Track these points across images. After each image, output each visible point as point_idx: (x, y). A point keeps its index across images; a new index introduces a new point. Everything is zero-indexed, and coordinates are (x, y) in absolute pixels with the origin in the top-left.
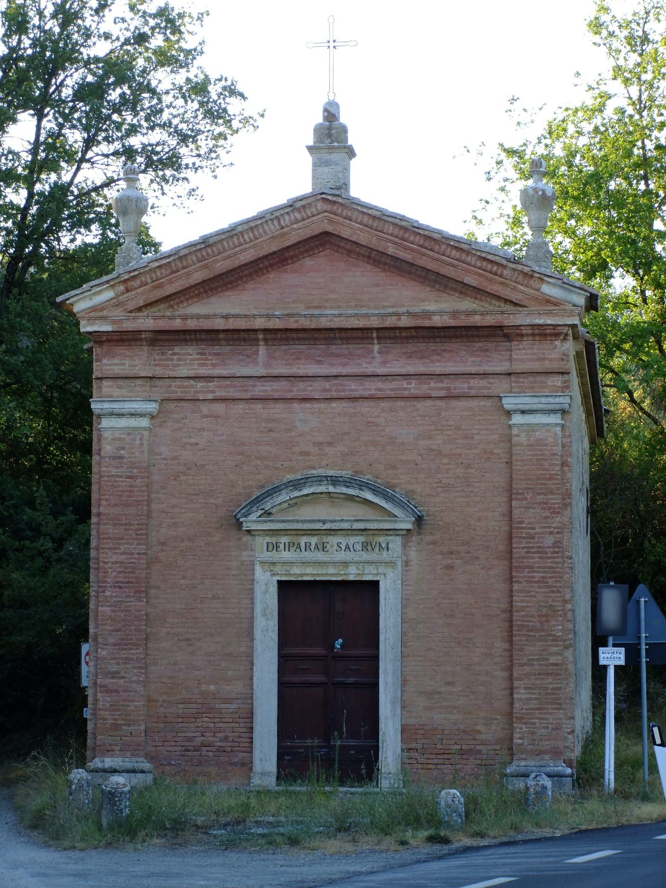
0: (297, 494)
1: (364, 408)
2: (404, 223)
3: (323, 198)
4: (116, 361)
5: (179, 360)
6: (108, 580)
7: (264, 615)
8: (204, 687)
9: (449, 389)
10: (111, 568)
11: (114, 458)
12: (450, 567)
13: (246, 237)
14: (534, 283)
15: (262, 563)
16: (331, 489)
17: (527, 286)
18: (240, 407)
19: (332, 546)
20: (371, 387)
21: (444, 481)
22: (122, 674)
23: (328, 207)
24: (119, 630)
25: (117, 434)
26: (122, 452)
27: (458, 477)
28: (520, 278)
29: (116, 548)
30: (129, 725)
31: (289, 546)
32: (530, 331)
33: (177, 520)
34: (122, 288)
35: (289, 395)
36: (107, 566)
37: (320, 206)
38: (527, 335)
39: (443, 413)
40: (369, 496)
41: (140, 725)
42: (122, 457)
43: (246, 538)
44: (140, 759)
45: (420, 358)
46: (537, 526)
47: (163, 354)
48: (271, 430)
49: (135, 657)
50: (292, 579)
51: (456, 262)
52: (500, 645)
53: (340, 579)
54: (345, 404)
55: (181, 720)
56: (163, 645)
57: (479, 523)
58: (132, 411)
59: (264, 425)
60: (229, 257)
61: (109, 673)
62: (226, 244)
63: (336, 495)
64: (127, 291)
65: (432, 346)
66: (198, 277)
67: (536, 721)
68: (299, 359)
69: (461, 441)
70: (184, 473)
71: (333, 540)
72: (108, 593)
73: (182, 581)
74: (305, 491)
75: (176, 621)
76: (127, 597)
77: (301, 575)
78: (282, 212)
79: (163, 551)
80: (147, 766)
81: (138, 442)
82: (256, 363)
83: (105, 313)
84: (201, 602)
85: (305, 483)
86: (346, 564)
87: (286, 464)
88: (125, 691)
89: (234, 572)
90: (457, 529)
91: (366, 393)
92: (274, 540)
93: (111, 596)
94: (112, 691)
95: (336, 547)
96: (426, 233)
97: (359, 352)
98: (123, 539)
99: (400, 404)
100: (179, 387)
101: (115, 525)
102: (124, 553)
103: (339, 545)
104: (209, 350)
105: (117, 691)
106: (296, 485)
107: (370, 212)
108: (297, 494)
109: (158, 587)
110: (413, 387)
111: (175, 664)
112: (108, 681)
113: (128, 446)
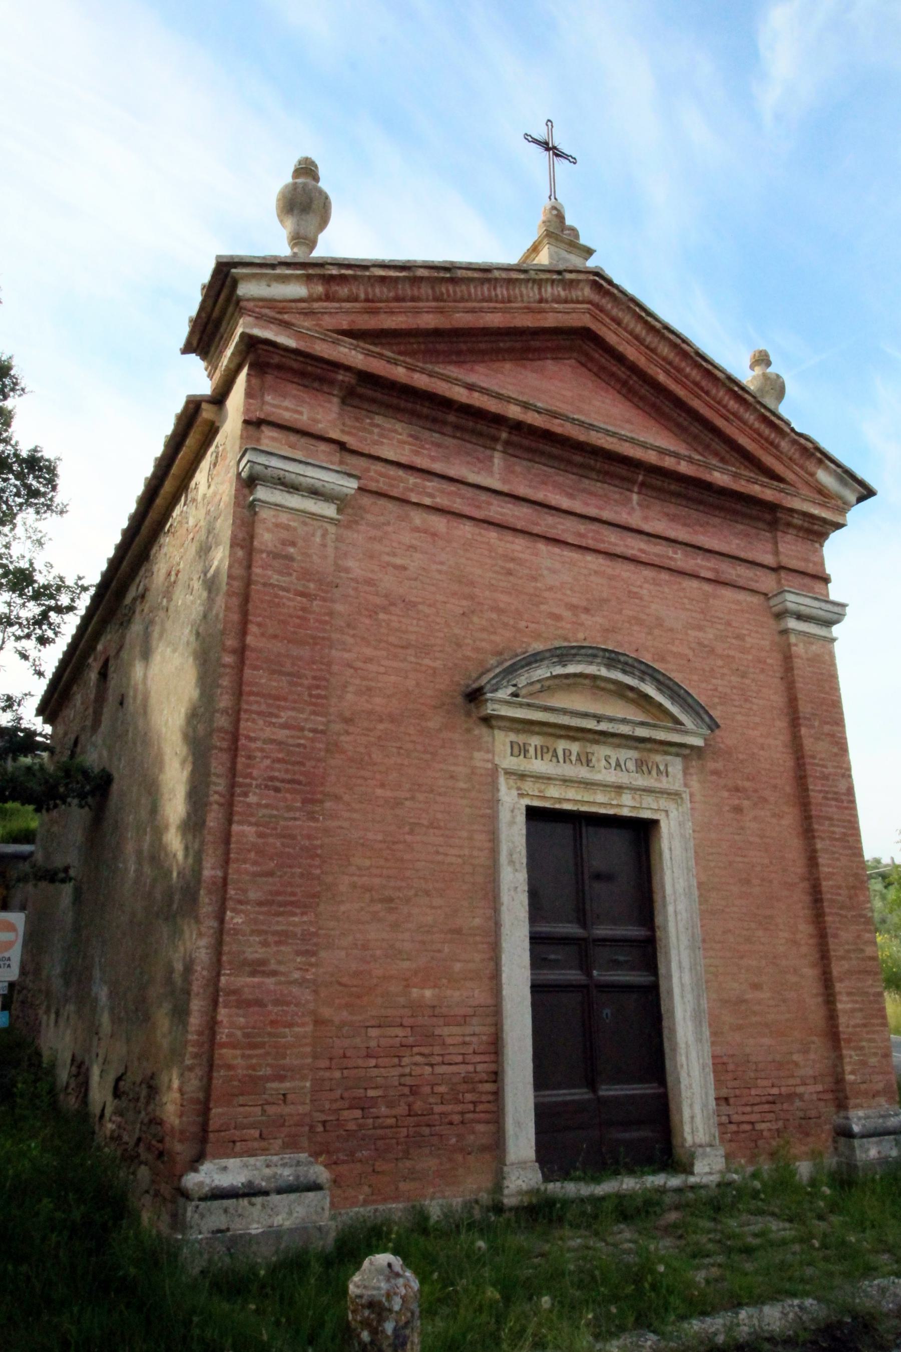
0: (559, 670)
1: (625, 571)
2: (684, 346)
3: (595, 282)
4: (287, 403)
5: (382, 436)
6: (255, 773)
7: (511, 862)
8: (415, 993)
9: (716, 571)
10: (262, 750)
11: (276, 556)
12: (738, 810)
13: (499, 291)
14: (811, 465)
15: (508, 773)
16: (604, 672)
17: (801, 467)
18: (467, 529)
19: (599, 760)
20: (634, 546)
21: (720, 689)
22: (273, 966)
23: (596, 298)
24: (271, 874)
25: (284, 518)
26: (292, 550)
27: (735, 687)
28: (797, 456)
29: (271, 715)
30: (281, 1078)
31: (542, 751)
32: (799, 522)
33: (373, 684)
34: (320, 289)
35: (536, 530)
36: (253, 745)
37: (587, 292)
38: (795, 527)
39: (711, 601)
40: (650, 689)
41: (303, 1078)
42: (290, 558)
43: (482, 731)
44: (303, 1156)
45: (685, 525)
46: (829, 764)
47: (357, 419)
48: (509, 573)
49: (298, 930)
50: (547, 804)
51: (731, 417)
52: (805, 929)
53: (611, 811)
54: (601, 560)
55: (373, 1062)
56: (343, 908)
57: (761, 753)
58: (318, 484)
59: (500, 562)
60: (472, 311)
61: (245, 963)
62: (473, 290)
63: (603, 684)
64: (328, 298)
65: (694, 514)
66: (429, 321)
67: (864, 1044)
68: (544, 483)
69: (734, 641)
70: (384, 609)
71: (601, 752)
72: (252, 799)
73: (379, 792)
74: (571, 669)
75: (367, 863)
76: (289, 809)
77: (560, 800)
78: (548, 276)
79: (348, 733)
80: (320, 1173)
81: (318, 539)
82: (491, 473)
83: (286, 317)
84: (411, 832)
85: (575, 655)
86: (619, 788)
87: (533, 626)
88: (277, 1002)
89: (462, 785)
90: (741, 757)
91: (629, 552)
92: (521, 739)
93: (259, 805)
94: (249, 1004)
95: (603, 763)
96: (710, 367)
97: (617, 497)
98: (285, 699)
99: (665, 576)
100: (381, 475)
101: (273, 672)
102: (285, 726)
103: (607, 759)
104: (426, 434)
105: (259, 1003)
106: (563, 655)
107: (649, 319)
108: (559, 670)
109: (337, 798)
110: (679, 558)
111: (365, 947)
112: (245, 981)
113: (300, 543)
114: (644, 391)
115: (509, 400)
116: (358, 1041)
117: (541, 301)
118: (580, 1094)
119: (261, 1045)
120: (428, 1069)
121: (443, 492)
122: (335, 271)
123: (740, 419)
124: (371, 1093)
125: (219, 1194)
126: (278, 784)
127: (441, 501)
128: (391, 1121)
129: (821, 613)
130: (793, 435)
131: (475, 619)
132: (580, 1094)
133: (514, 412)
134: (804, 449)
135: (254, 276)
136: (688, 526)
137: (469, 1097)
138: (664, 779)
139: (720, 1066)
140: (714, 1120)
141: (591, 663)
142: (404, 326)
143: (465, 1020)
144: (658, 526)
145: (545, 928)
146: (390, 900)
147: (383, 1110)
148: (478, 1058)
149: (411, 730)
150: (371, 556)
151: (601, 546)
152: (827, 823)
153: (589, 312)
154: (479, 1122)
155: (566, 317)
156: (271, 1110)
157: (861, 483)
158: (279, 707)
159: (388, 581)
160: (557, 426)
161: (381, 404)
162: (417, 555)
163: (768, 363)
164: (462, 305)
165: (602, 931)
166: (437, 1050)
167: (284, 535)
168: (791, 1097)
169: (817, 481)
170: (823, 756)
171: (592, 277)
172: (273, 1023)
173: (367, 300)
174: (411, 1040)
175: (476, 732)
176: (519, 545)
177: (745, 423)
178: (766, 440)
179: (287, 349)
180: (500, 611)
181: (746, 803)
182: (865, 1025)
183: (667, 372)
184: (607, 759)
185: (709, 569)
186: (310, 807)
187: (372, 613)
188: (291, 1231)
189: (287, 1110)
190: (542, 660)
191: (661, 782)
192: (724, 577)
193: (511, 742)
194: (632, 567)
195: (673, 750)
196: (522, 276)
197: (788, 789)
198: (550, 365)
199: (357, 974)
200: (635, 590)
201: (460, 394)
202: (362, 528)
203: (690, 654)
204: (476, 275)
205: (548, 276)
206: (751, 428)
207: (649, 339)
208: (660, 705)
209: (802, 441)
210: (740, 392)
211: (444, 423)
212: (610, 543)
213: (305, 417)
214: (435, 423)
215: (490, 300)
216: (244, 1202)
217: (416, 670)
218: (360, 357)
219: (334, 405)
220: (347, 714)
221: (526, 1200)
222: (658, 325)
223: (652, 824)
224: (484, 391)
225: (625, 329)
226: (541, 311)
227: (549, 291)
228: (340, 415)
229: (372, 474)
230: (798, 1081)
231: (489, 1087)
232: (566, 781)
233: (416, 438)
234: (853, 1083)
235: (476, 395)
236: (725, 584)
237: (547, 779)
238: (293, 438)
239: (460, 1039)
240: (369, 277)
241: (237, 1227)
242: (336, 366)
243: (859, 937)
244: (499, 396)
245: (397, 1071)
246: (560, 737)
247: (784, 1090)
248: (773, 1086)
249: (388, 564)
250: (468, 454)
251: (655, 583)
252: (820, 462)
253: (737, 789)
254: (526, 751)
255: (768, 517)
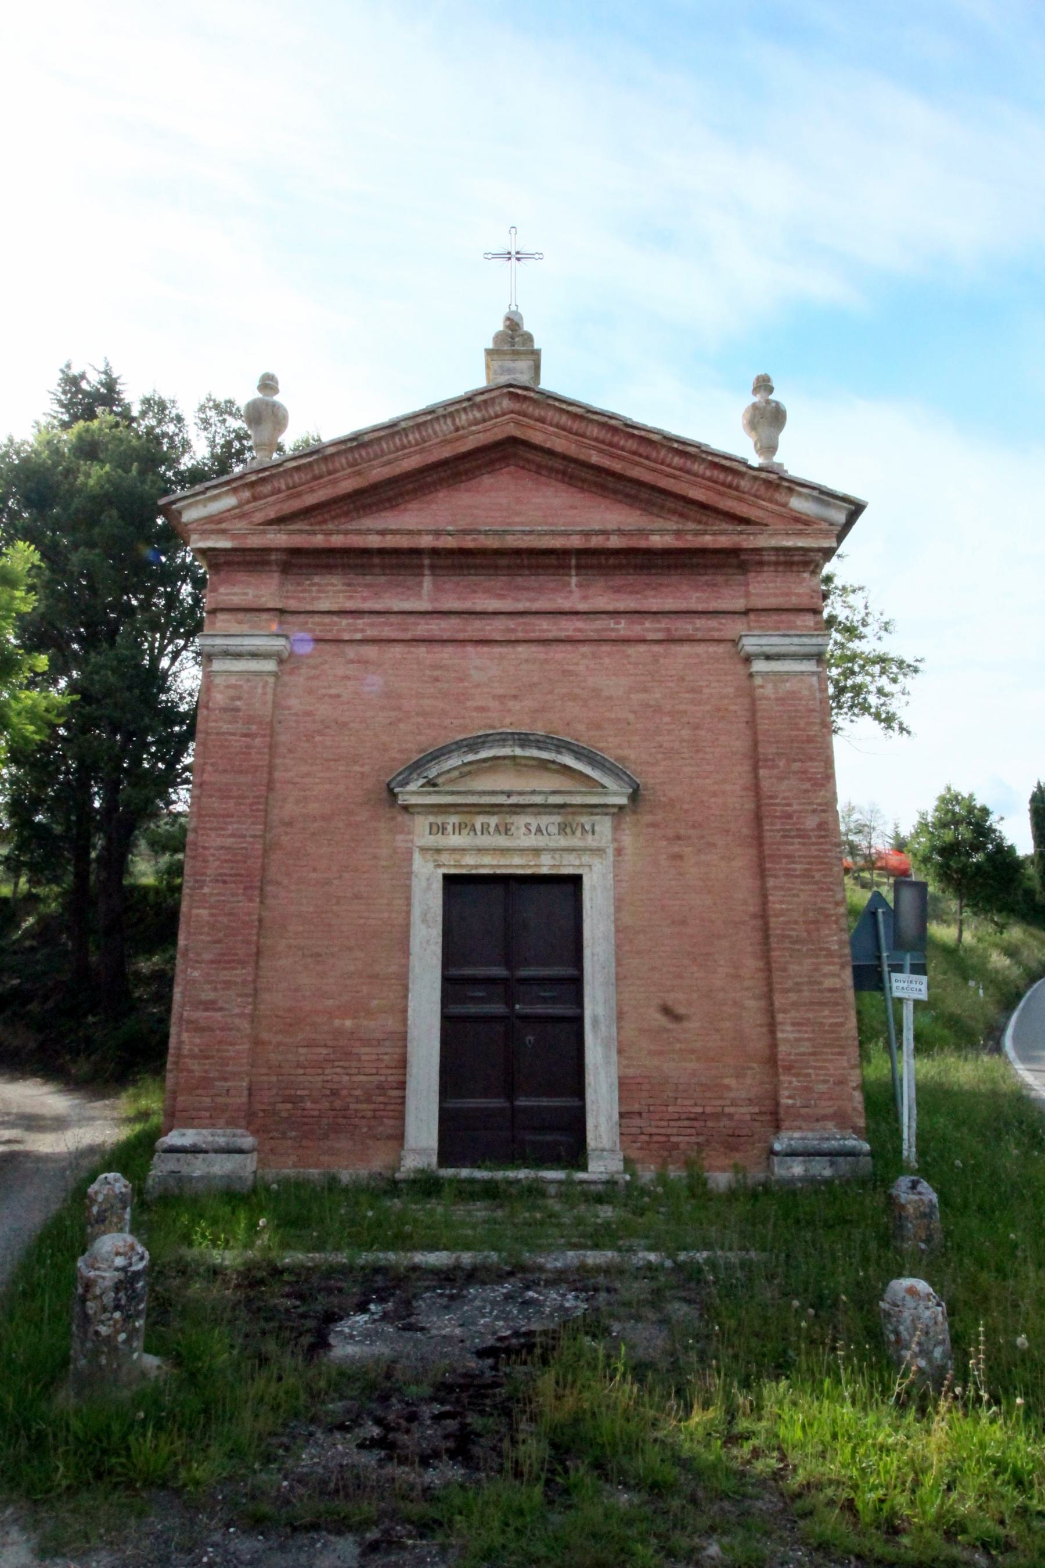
0: (471, 757)
1: (560, 653)
2: (613, 422)
3: (510, 393)
4: (236, 590)
5: (319, 591)
6: (209, 872)
7: (424, 921)
8: (337, 1022)
9: (668, 630)
10: (213, 855)
11: (225, 710)
12: (679, 857)
13: (411, 437)
14: (779, 497)
15: (423, 850)
16: (518, 752)
17: (770, 501)
18: (397, 650)
19: (518, 828)
20: (569, 627)
21: (665, 744)
22: (220, 1004)
23: (517, 406)
24: (219, 941)
25: (233, 680)
26: (238, 703)
27: (684, 741)
28: (762, 491)
29: (223, 829)
30: (225, 1079)
31: (459, 828)
32: (773, 558)
33: (308, 793)
34: (247, 494)
35: (461, 636)
36: (207, 852)
37: (506, 404)
38: (769, 563)
39: (662, 661)
40: (569, 760)
41: (242, 1079)
42: (237, 710)
43: (402, 818)
44: (239, 1131)
45: (631, 593)
46: (795, 802)
47: (299, 584)
48: (437, 679)
49: (239, 980)
50: (464, 871)
51: (678, 473)
52: (751, 964)
53: (529, 871)
54: (534, 648)
55: (301, 1071)
56: (281, 962)
57: (713, 800)
58: (253, 649)
59: (428, 672)
60: (389, 463)
61: (201, 1002)
62: (385, 446)
63: (523, 762)
64: (255, 498)
65: (645, 579)
66: (347, 486)
67: (810, 1071)
68: (474, 592)
69: (687, 695)
70: (320, 733)
71: (520, 821)
72: (206, 890)
73: (314, 875)
74: (484, 754)
75: (301, 928)
76: (233, 895)
77: (477, 867)
78: (457, 407)
79: (286, 833)
80: (248, 1141)
81: (260, 691)
82: (419, 596)
83: (224, 526)
84: (338, 903)
85: (484, 743)
86: (537, 851)
87: (456, 722)
88: (222, 1029)
89: (384, 863)
90: (686, 806)
91: (563, 635)
92: (439, 820)
93: (211, 894)
94: (203, 1030)
95: (523, 830)
96: (643, 433)
97: (552, 585)
98: (232, 816)
99: (606, 648)
100: (318, 624)
101: (222, 798)
102: (232, 835)
103: (527, 826)
104: (360, 579)
105: (210, 1029)
106: (473, 744)
107: (570, 408)
108: (471, 757)
109: (278, 883)
110: (622, 627)
111: (296, 990)
112: (199, 1015)
113: (246, 696)
114: (584, 474)
115: (419, 533)
116: (290, 1057)
117: (457, 429)
118: (496, 1103)
119: (212, 1057)
120: (346, 1078)
121: (372, 625)
122: (253, 478)
123: (688, 472)
124: (299, 1093)
125: (172, 1150)
126: (225, 878)
127: (370, 633)
128: (316, 1113)
129: (793, 649)
130: (751, 472)
131: (402, 726)
132: (496, 1103)
133: (426, 542)
134: (768, 483)
135: (190, 505)
136: (637, 593)
137: (381, 1099)
138: (590, 837)
139: (625, 1086)
140: (617, 1130)
141: (504, 746)
142: (323, 499)
143: (379, 1042)
144: (603, 602)
145: (454, 972)
146: (318, 955)
147: (309, 1105)
148: (390, 1071)
149: (341, 825)
150: (310, 692)
151: (533, 635)
152: (784, 861)
153: (513, 420)
154: (389, 1118)
155: (488, 434)
156: (219, 1100)
157: (845, 499)
158: (226, 823)
159: (324, 710)
160: (469, 543)
161: (316, 566)
162: (349, 683)
163: (771, 390)
164: (375, 463)
165: (524, 972)
166: (354, 1064)
167: (232, 692)
168: (716, 1116)
169: (791, 510)
170: (787, 794)
171: (505, 390)
172: (220, 1042)
173: (289, 488)
174: (332, 1057)
175: (399, 819)
176: (446, 654)
177: (696, 475)
178: (723, 484)
179: (225, 550)
180: (424, 714)
181: (688, 850)
182: (814, 1054)
183: (601, 451)
184: (527, 826)
185: (659, 630)
186: (249, 892)
187: (309, 737)
188: (222, 1177)
189: (229, 1100)
190: (452, 751)
191: (585, 839)
192: (678, 634)
193: (431, 825)
194: (569, 647)
195: (598, 810)
196: (429, 417)
197: (745, 831)
198: (487, 480)
199: (290, 1010)
200: (571, 668)
201: (374, 541)
202: (304, 671)
203: (631, 717)
204: (387, 431)
205: (457, 407)
206: (703, 477)
207: (576, 426)
208: (581, 773)
209: (764, 475)
210: (681, 447)
211: (373, 566)
212: (544, 631)
213: (250, 597)
214: (363, 569)
215: (404, 447)
216: (189, 1156)
217: (346, 777)
218: (284, 537)
219: (275, 578)
220: (287, 820)
221: (412, 1176)
222: (579, 411)
223: (576, 881)
224: (394, 532)
225: (551, 425)
226: (463, 437)
227: (463, 419)
228: (282, 584)
229: (310, 626)
230: (728, 1102)
231: (397, 1093)
232: (480, 850)
233: (349, 585)
234: (788, 1107)
235: (389, 537)
236: (681, 641)
237: (463, 850)
238: (241, 616)
239: (374, 1057)
240: (285, 471)
241: (185, 1170)
242: (267, 550)
243: (816, 970)
244: (410, 532)
245: (319, 1078)
246: (479, 813)
247: (708, 1110)
248: (696, 1105)
249: (324, 696)
250: (398, 586)
251: (594, 656)
252: (790, 490)
253: (678, 838)
254: (444, 829)
255: (734, 561)
